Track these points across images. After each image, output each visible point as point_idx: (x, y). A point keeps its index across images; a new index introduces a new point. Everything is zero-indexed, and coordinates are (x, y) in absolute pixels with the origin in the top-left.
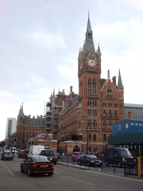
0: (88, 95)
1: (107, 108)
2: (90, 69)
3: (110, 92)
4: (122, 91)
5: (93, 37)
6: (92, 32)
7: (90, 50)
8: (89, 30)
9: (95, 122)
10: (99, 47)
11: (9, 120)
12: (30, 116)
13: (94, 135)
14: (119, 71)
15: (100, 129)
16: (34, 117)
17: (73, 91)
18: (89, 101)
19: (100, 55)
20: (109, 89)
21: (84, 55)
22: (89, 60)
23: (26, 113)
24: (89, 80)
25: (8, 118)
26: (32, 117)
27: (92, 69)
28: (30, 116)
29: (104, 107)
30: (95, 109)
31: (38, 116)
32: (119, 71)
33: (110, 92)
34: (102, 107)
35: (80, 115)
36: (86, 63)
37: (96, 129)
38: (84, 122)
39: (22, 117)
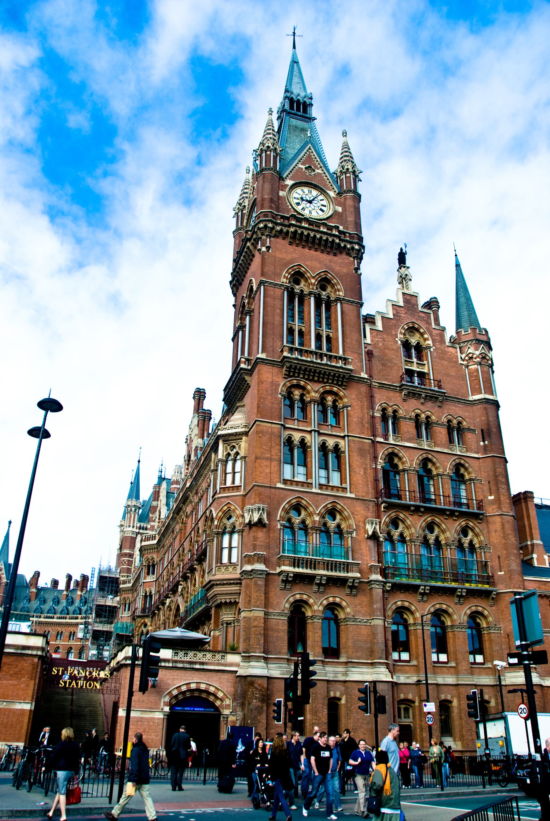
0: (291, 350)
1: (409, 440)
8: (296, 90)
9: (332, 525)
13: (332, 607)
14: (458, 266)
15: (371, 569)
16: (55, 583)
17: (205, 407)
18: (297, 393)
20: (413, 341)
26: (44, 582)
28: (37, 575)
29: (386, 437)
30: (331, 443)
31: (69, 577)
32: (458, 266)
33: (419, 358)
34: (374, 436)
35: (229, 477)
36: (279, 197)
37: (347, 567)
38: (256, 519)
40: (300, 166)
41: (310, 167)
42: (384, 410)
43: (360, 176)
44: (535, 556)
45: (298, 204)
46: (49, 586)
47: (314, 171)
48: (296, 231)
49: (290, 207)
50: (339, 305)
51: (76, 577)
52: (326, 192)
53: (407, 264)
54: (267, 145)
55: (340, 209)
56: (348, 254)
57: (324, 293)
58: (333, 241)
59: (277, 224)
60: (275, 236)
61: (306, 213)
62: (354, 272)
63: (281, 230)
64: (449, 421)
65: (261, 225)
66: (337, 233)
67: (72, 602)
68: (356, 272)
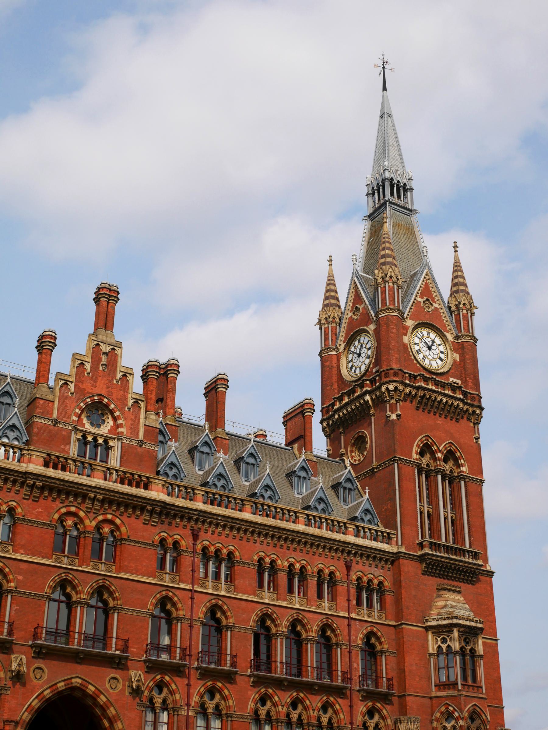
0: (433, 545)
5: (414, 208)
10: (457, 267)
19: (471, 309)
21: (392, 290)
22: (416, 327)
24: (422, 454)
40: (419, 299)
41: (427, 300)
43: (475, 311)
45: (419, 352)
47: (432, 305)
48: (425, 395)
49: (412, 357)
50: (463, 483)
52: (445, 335)
54: (389, 274)
55: (457, 357)
56: (469, 419)
57: (447, 467)
58: (458, 405)
59: (406, 385)
60: (405, 400)
61: (427, 362)
62: (475, 441)
63: (410, 392)
65: (391, 387)
66: (461, 397)
68: (477, 442)
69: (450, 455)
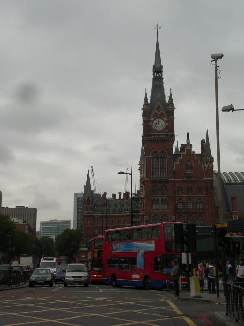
2: (154, 135)
3: (191, 169)
4: (209, 166)
6: (161, 67)
7: (156, 103)
10: (171, 97)
11: (78, 199)
12: (105, 194)
16: (114, 195)
23: (98, 189)
25: (74, 193)
26: (109, 196)
27: (158, 135)
28: (105, 194)
30: (164, 198)
31: (120, 193)
33: (191, 169)
39: (89, 198)
42: (178, 187)
44: (233, 216)
46: (111, 197)
51: (123, 192)
53: (189, 138)
64: (197, 187)
67: (123, 205)
69: (163, 152)
